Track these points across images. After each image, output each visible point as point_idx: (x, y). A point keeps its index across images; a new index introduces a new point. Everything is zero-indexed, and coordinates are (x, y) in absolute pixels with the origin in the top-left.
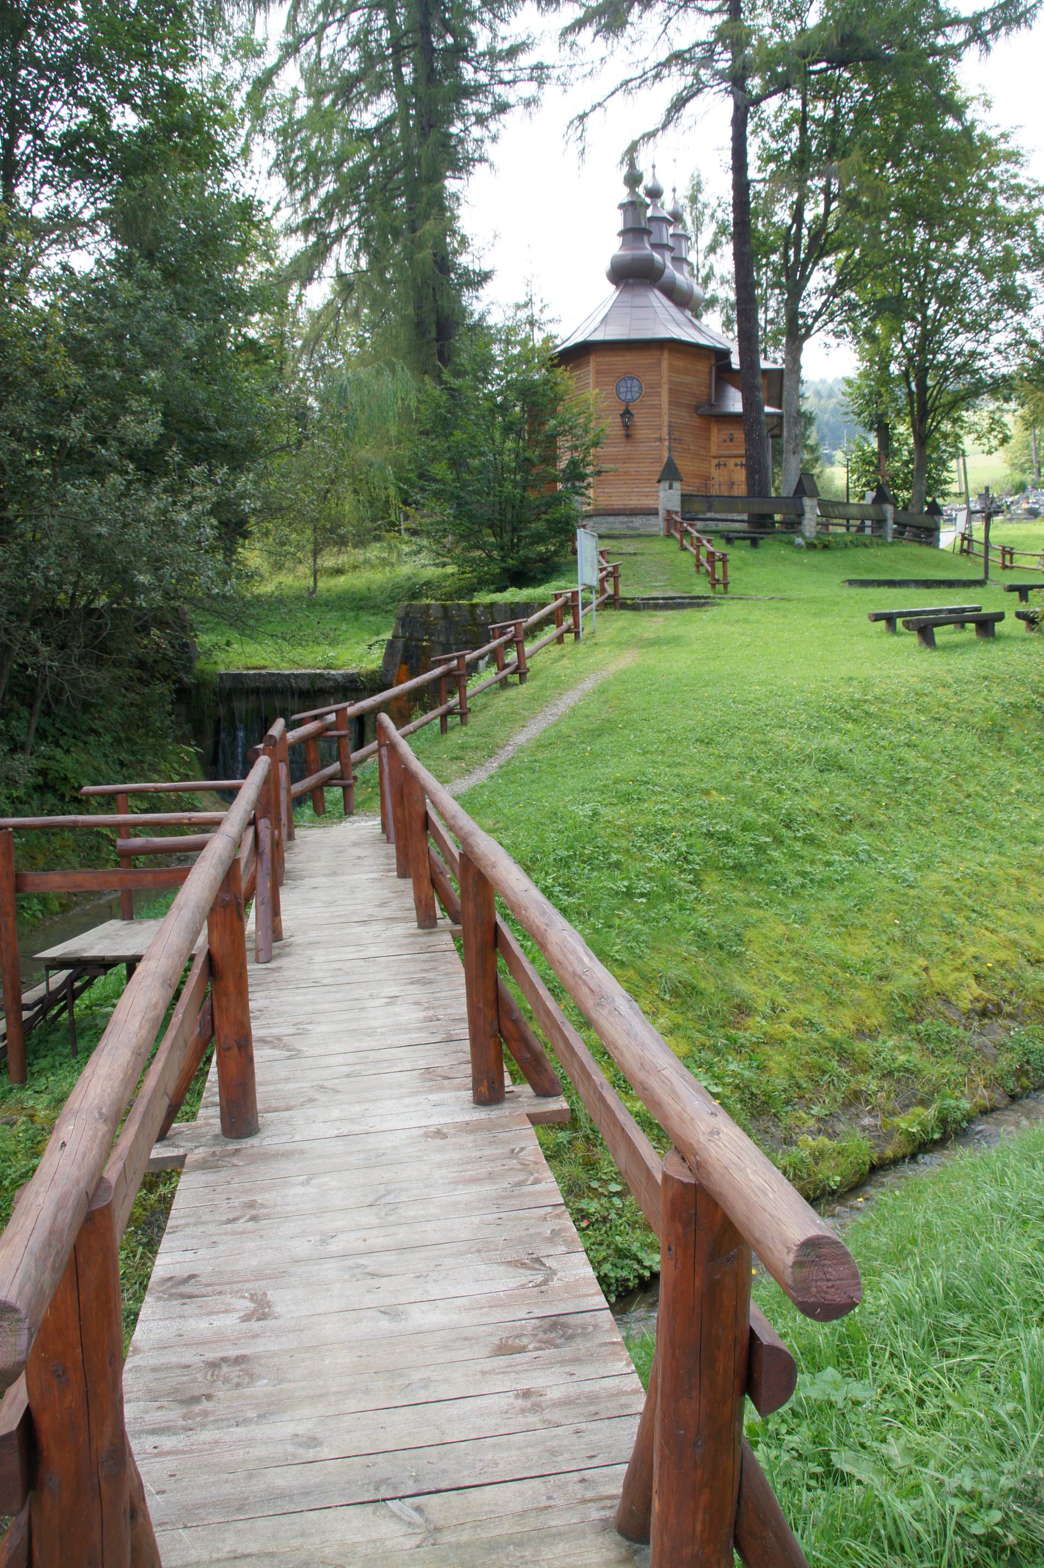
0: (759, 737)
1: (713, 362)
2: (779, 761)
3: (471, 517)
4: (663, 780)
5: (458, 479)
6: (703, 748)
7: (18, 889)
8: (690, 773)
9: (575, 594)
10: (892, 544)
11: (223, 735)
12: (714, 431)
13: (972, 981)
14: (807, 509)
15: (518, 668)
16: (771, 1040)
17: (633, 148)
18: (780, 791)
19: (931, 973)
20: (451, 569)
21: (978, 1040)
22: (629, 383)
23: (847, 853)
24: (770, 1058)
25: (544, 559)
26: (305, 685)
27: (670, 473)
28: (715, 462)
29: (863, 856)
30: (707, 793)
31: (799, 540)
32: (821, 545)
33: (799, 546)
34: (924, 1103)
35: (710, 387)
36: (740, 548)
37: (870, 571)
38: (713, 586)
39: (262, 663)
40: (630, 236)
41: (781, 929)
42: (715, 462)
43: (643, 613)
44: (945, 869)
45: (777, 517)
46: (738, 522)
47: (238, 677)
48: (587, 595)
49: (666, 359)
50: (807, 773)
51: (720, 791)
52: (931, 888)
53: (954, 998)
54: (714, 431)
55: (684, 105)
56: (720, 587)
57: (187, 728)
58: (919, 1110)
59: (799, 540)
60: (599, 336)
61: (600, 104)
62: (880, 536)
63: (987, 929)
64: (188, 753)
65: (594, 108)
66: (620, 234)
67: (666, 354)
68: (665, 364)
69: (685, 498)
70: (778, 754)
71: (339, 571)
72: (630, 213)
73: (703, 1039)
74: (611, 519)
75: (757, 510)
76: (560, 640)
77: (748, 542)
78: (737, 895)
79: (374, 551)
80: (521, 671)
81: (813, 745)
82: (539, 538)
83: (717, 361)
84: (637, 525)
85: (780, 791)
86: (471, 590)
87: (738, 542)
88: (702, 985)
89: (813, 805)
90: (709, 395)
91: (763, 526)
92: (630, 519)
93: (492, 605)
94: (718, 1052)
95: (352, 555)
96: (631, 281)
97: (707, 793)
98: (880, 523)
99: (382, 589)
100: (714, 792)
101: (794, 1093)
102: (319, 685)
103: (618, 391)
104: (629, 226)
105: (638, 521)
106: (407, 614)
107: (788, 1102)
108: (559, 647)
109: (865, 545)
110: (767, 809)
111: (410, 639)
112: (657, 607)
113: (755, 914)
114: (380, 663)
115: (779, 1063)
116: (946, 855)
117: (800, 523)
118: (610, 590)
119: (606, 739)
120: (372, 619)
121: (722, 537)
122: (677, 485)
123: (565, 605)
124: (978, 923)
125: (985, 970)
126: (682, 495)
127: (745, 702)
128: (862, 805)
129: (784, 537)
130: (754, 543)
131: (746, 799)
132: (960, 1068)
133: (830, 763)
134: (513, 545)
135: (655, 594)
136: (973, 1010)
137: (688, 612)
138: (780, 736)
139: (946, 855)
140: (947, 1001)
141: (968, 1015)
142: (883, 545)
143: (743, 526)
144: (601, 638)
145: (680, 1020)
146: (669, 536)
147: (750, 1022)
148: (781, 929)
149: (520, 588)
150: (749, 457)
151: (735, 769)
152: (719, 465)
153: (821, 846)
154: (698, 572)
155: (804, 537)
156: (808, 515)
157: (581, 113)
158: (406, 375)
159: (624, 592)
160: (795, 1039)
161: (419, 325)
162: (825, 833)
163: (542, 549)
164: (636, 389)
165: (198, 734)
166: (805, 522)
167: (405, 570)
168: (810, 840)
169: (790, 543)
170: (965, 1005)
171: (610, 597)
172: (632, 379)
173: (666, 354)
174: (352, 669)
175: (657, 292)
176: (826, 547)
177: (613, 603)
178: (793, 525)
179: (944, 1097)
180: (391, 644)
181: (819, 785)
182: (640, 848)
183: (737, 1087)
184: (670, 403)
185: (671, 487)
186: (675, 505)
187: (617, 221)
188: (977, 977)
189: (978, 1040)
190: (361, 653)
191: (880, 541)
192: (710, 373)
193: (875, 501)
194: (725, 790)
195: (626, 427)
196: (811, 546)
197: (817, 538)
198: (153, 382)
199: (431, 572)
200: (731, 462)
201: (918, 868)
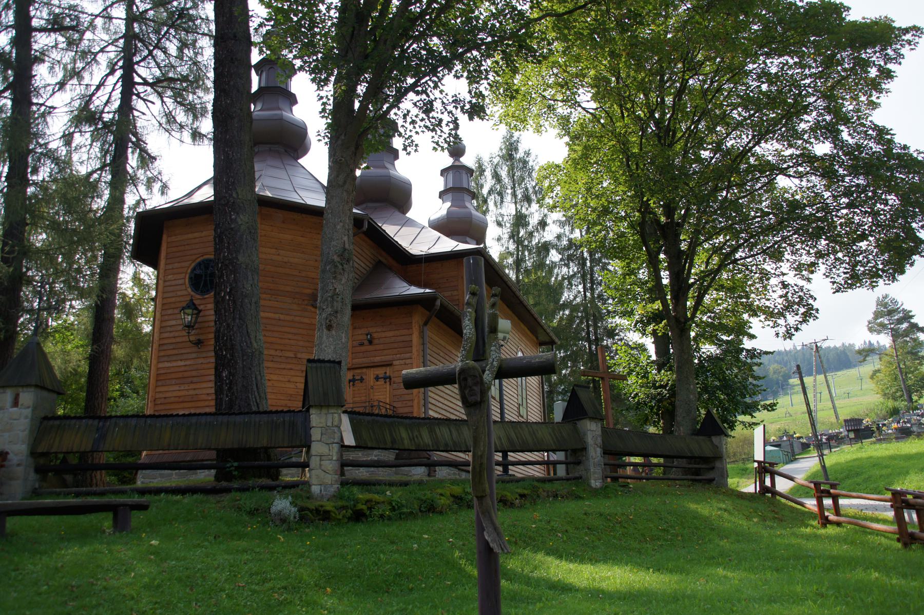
10: (595, 493)
152: (353, 381)
169: (260, 512)
176: (358, 516)
185: (16, 403)
193: (567, 415)
196: (313, 516)
200: (371, 374)
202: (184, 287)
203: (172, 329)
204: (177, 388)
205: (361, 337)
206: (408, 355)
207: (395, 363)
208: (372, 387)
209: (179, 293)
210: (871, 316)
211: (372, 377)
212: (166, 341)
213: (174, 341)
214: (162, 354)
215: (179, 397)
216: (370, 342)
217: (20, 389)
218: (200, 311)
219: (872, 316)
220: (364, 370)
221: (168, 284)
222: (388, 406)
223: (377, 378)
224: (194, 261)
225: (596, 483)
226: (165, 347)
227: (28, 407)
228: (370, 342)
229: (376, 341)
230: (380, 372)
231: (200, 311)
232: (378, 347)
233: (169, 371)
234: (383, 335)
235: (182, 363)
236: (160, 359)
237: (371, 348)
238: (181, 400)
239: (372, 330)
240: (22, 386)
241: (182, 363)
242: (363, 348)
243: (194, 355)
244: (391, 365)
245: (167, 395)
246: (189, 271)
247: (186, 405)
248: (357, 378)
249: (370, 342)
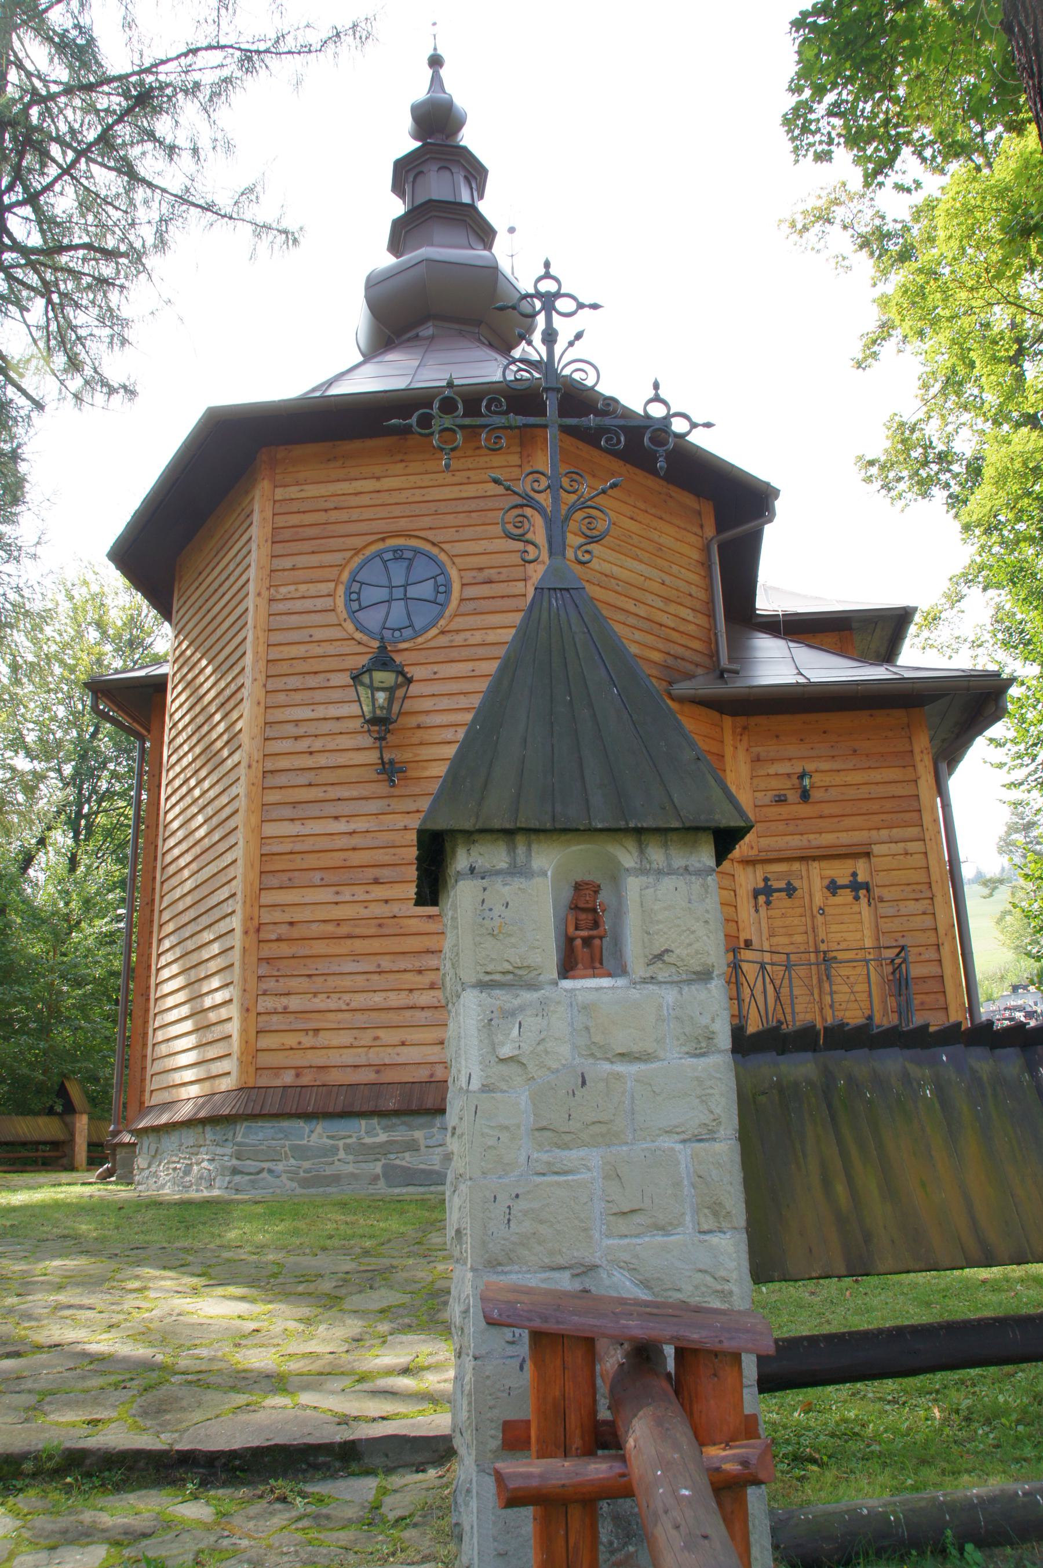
1: (710, 531)
35: (711, 615)
74: (317, 1135)
90: (711, 641)
92: (401, 1133)
103: (353, 597)
122: (670, 903)
126: (743, 1044)
152: (764, 892)
185: (586, 940)
195: (381, 724)
200: (814, 878)
202: (331, 618)
203: (300, 731)
204: (326, 895)
205: (775, 783)
206: (913, 831)
207: (876, 849)
208: (822, 910)
209: (319, 634)
210: (1002, 830)
212: (284, 763)
213: (309, 762)
214: (272, 797)
215: (338, 922)
216: (805, 796)
217: (626, 856)
218: (409, 681)
219: (1005, 829)
220: (796, 866)
221: (281, 607)
222: (767, 957)
223: (833, 887)
224: (358, 551)
226: (281, 780)
227: (704, 976)
229: (816, 795)
230: (841, 871)
231: (409, 681)
232: (827, 809)
233: (298, 847)
234: (838, 779)
235: (342, 826)
236: (265, 812)
237: (804, 810)
238: (344, 930)
239: (810, 767)
240: (640, 833)
241: (342, 826)
242: (784, 810)
243: (373, 807)
244: (868, 855)
245: (298, 915)
246: (345, 576)
247: (359, 945)
248: (776, 885)
249: (805, 796)
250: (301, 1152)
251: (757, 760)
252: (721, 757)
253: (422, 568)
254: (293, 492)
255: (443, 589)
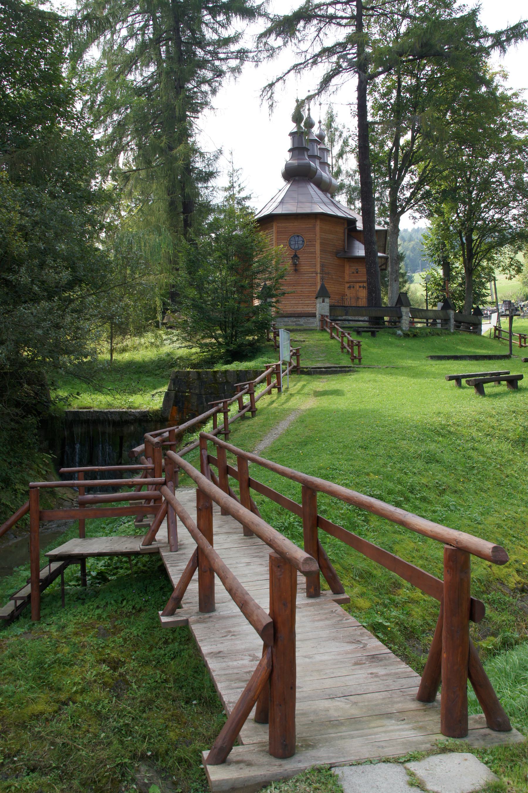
0: (393, 445)
1: (346, 226)
2: (404, 457)
3: (209, 320)
4: (344, 468)
5: (201, 298)
6: (363, 451)
7: (41, 519)
8: (358, 464)
9: (278, 366)
10: (453, 334)
11: (67, 448)
12: (347, 267)
13: (515, 573)
14: (404, 314)
15: (251, 408)
16: (412, 601)
17: (300, 105)
18: (406, 473)
19: (493, 568)
20: (194, 350)
21: (520, 604)
22: (296, 238)
23: (443, 506)
24: (412, 610)
25: (251, 344)
26: (117, 418)
27: (323, 293)
28: (347, 285)
29: (452, 508)
30: (368, 474)
31: (399, 332)
32: (413, 335)
33: (399, 336)
34: (495, 635)
36: (365, 337)
37: (442, 350)
38: (353, 360)
39: (88, 405)
40: (296, 152)
41: (412, 545)
42: (347, 285)
43: (314, 376)
44: (497, 515)
45: (386, 318)
46: (363, 321)
47: (76, 413)
48: (284, 367)
49: (318, 225)
50: (420, 464)
51: (375, 474)
52: (490, 525)
53: (506, 582)
54: (347, 267)
55: (330, 80)
56: (357, 361)
57: (46, 444)
58: (492, 638)
59: (399, 332)
60: (279, 211)
61: (281, 78)
62: (446, 329)
63: (521, 546)
64: (47, 458)
65: (278, 80)
66: (289, 151)
67: (318, 222)
68: (318, 228)
69: (332, 308)
70: (404, 454)
71: (124, 350)
72: (296, 138)
73: (377, 600)
74: (286, 319)
75: (374, 315)
76: (269, 392)
77: (370, 333)
78: (387, 527)
79: (149, 337)
80: (253, 410)
81: (422, 449)
82: (250, 332)
83: (348, 226)
84: (302, 323)
85: (406, 473)
86: (211, 362)
87: (363, 334)
88: (375, 572)
89: (424, 481)
91: (378, 324)
93: (226, 371)
94: (385, 606)
95: (129, 341)
96: (297, 178)
97: (368, 474)
98: (446, 321)
99: (152, 362)
100: (371, 474)
101: (426, 627)
102: (125, 418)
104: (296, 146)
105: (302, 321)
106: (177, 377)
107: (423, 632)
108: (269, 396)
109: (438, 334)
110: (400, 483)
111: (178, 392)
112: (322, 373)
113: (398, 537)
114: (161, 405)
115: (417, 612)
116: (497, 507)
117: (400, 322)
118: (294, 363)
119: (309, 447)
120: (148, 379)
121: (354, 331)
122: (327, 300)
123: (272, 372)
124: (516, 543)
125: (522, 567)
127: (384, 426)
128: (450, 480)
129: (391, 330)
130: (373, 334)
131: (389, 477)
132: (512, 618)
133: (431, 459)
134: (232, 336)
135: (319, 365)
136: (517, 588)
137: (339, 376)
138: (404, 444)
139: (497, 507)
140: (502, 584)
141: (514, 590)
142: (448, 334)
143: (367, 324)
144: (292, 390)
145: (364, 590)
146: (323, 330)
147: (400, 591)
148: (412, 545)
149: (241, 362)
150: (369, 284)
151: (381, 462)
152: (350, 287)
153: (429, 502)
154: (343, 352)
155: (402, 330)
156: (404, 317)
157: (270, 83)
158: (168, 235)
159: (303, 364)
160: (425, 601)
161: (172, 204)
162: (432, 496)
163: (251, 338)
164: (301, 242)
165: (51, 447)
166: (403, 321)
167: (167, 349)
168: (424, 499)
169: (394, 334)
170: (512, 585)
171: (294, 367)
172: (298, 236)
173: (318, 222)
174: (145, 408)
175: (312, 185)
176: (415, 336)
177: (297, 371)
178: (396, 323)
179: (504, 632)
180: (167, 394)
181: (426, 470)
182: (336, 503)
183: (397, 623)
184: (321, 251)
186: (326, 311)
187: (288, 143)
188: (518, 571)
189: (520, 604)
190: (150, 400)
191: (447, 332)
192: (344, 233)
193: (443, 308)
194: (378, 473)
195: (295, 265)
196: (406, 336)
197: (410, 331)
198: (62, 250)
199: (183, 352)
200: (358, 285)
201: (482, 514)
211: (358, 286)
216: (357, 273)
223: (360, 287)
225: (452, 331)
228: (357, 273)
250: (284, 322)
251: (350, 266)
252: (344, 266)
253: (300, 239)
254: (280, 225)
255: (303, 241)
